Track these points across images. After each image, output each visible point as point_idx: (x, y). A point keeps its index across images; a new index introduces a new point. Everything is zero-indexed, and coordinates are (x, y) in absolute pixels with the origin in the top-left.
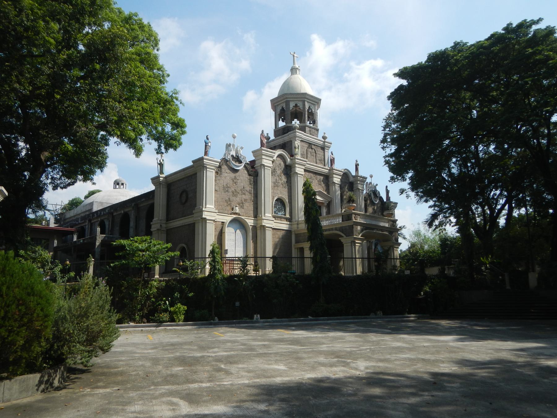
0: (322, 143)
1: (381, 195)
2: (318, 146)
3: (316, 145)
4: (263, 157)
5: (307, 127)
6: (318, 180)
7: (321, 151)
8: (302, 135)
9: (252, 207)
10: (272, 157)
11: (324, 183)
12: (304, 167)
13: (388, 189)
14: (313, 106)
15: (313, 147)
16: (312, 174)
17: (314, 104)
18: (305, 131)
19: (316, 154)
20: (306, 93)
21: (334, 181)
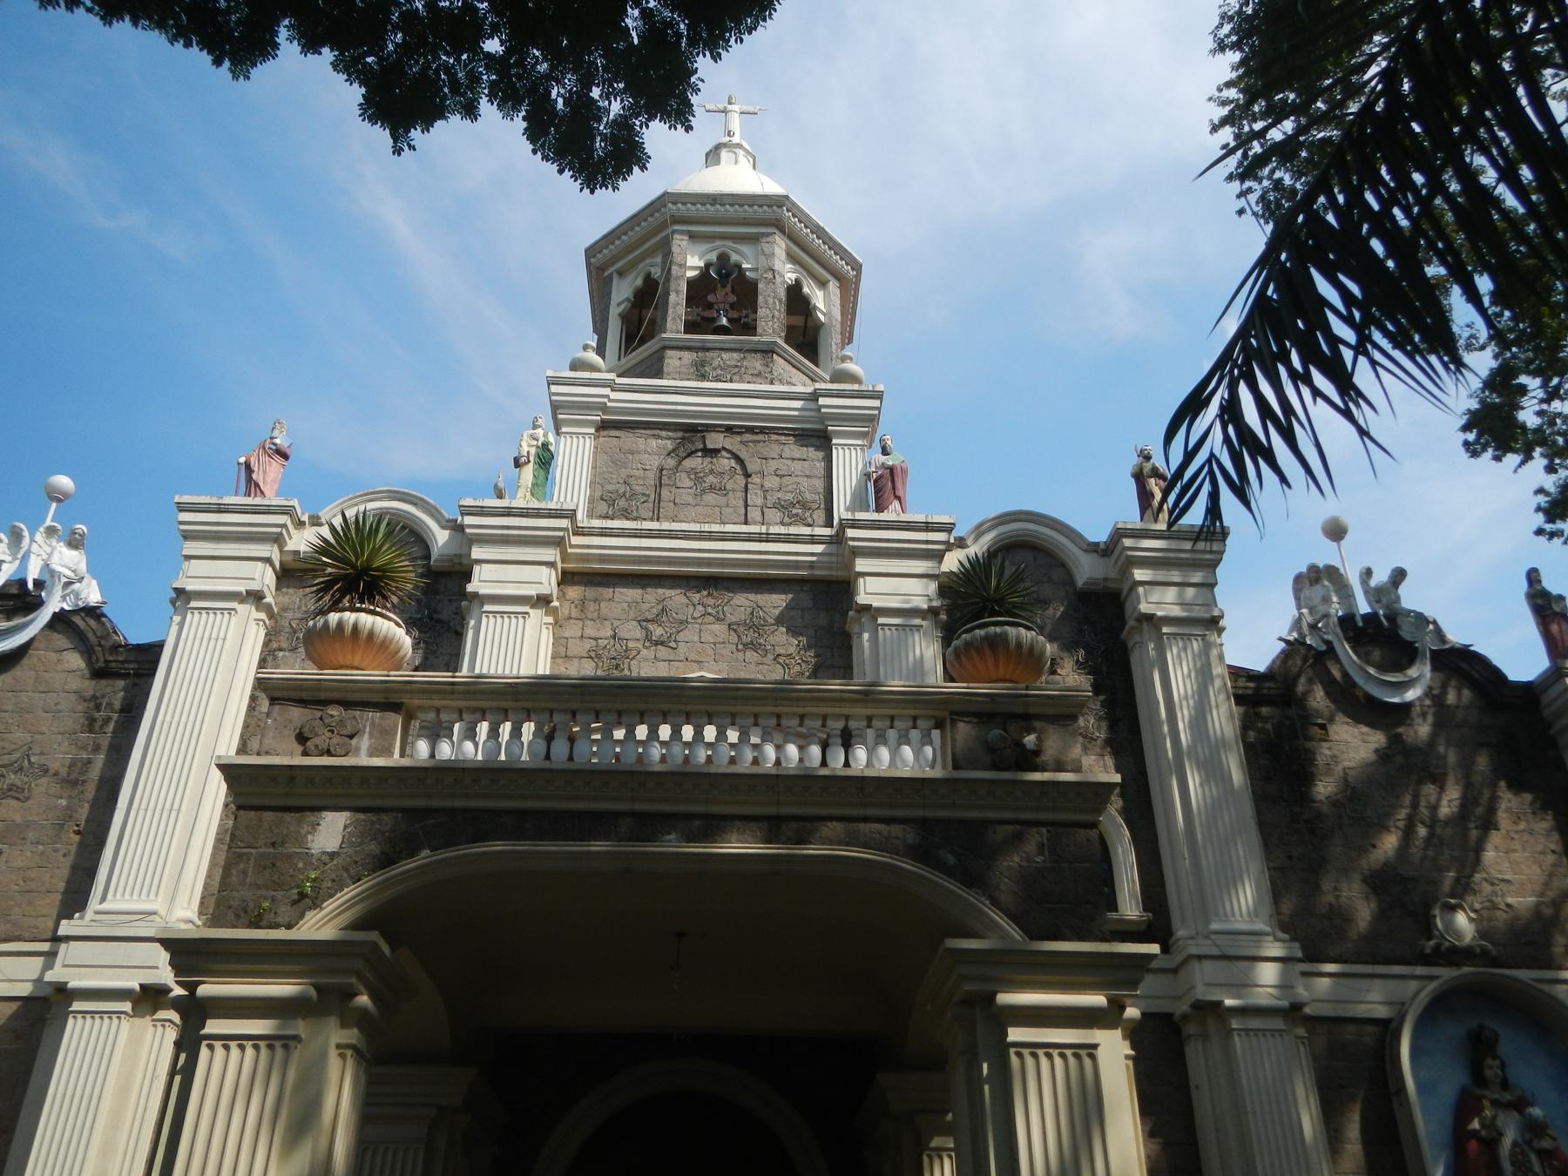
0: (798, 404)
1: (1457, 635)
2: (763, 430)
3: (751, 430)
4: (192, 548)
5: (669, 353)
6: (731, 618)
7: (793, 449)
8: (606, 391)
9: (64, 872)
10: (277, 540)
11: (793, 631)
12: (551, 554)
13: (1551, 584)
14: (746, 249)
15: (715, 440)
16: (668, 592)
17: (754, 239)
18: (658, 374)
19: (747, 475)
20: (665, 194)
21: (862, 599)
